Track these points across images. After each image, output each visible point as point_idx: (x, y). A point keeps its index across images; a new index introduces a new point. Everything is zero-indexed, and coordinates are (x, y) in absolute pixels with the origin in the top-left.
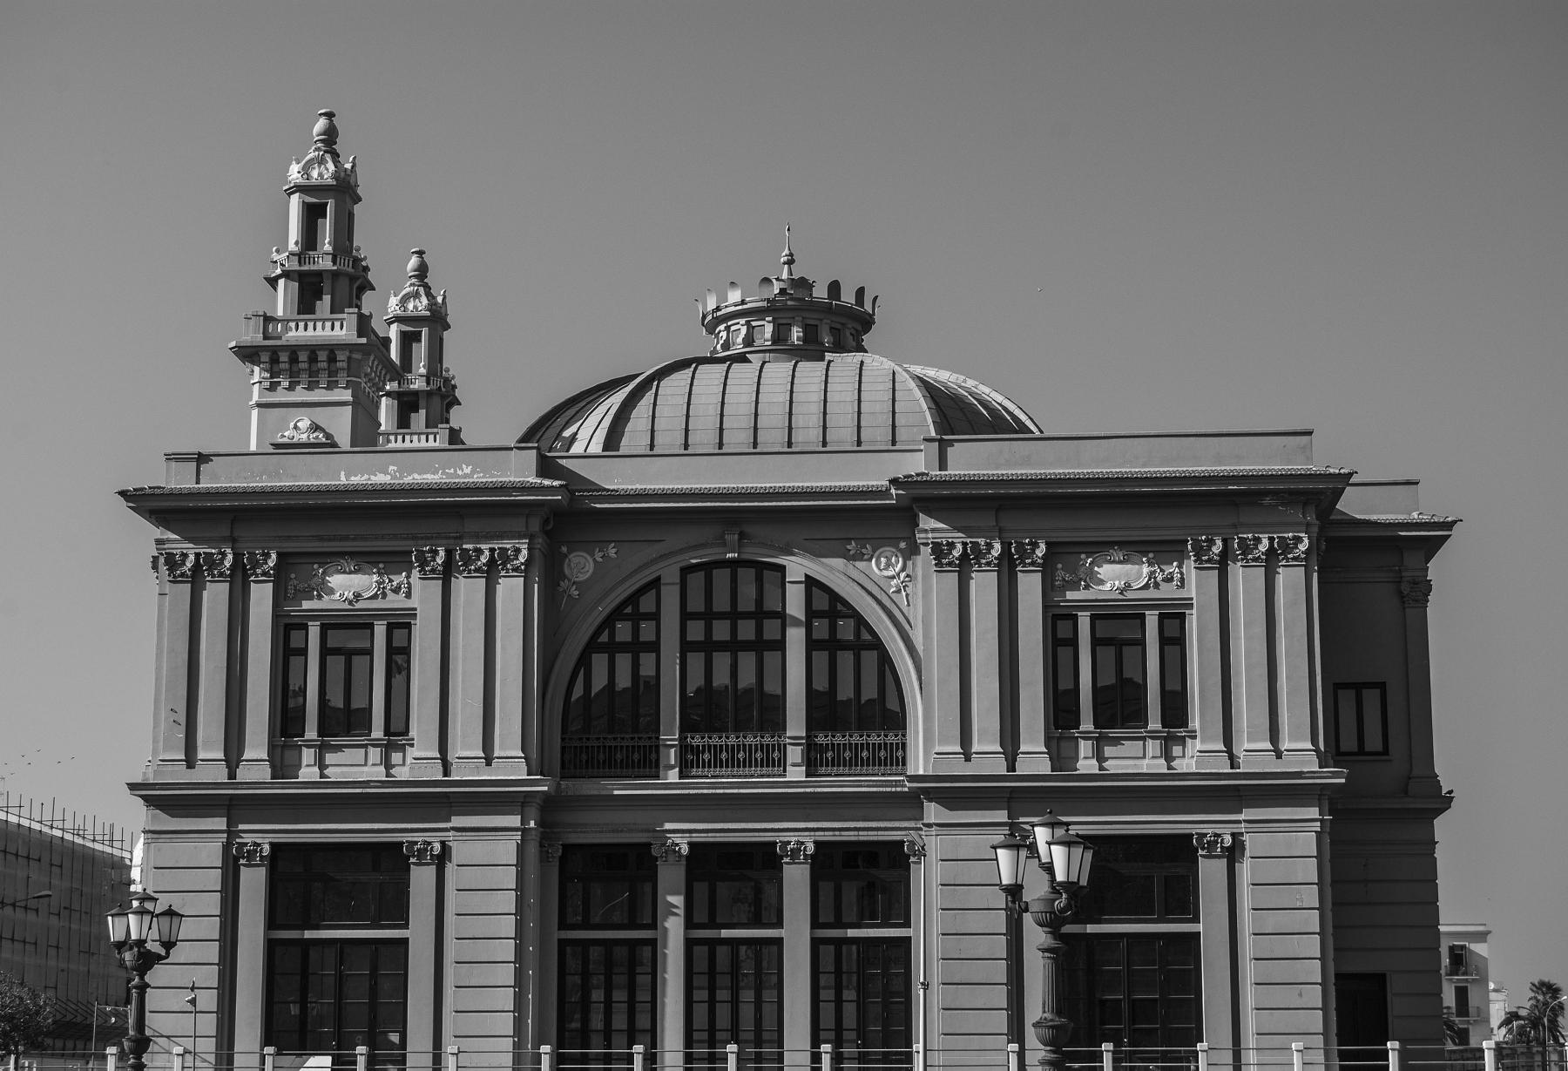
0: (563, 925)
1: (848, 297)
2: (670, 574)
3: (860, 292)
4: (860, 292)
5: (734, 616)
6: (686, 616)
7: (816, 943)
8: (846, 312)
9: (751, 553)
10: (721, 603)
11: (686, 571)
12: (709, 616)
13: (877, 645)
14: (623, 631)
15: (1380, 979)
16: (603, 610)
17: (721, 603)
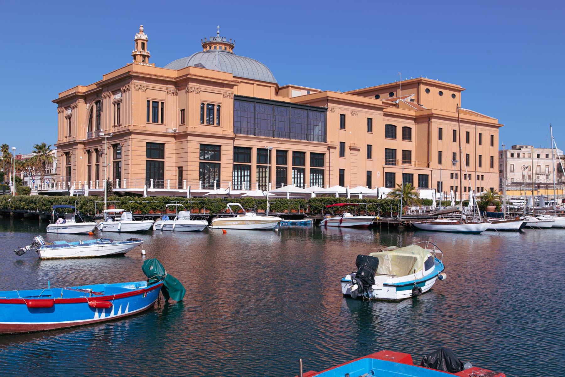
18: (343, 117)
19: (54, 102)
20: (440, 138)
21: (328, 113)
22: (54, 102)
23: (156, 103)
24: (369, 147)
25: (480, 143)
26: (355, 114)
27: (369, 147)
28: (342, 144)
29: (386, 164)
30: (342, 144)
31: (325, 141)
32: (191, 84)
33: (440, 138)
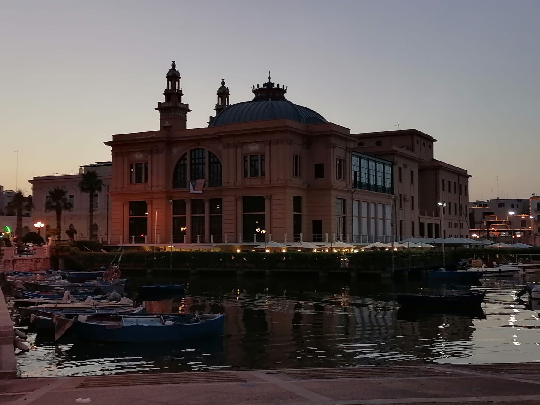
0: (174, 214)
1: (281, 87)
2: (188, 152)
3: (283, 86)
4: (283, 86)
5: (199, 158)
6: (191, 158)
7: (174, 218)
8: (281, 90)
9: (200, 147)
10: (197, 156)
11: (191, 151)
12: (195, 159)
13: (220, 163)
14: (182, 162)
15: (321, 221)
16: (177, 160)
17: (197, 156)
18: (400, 169)
19: (107, 143)
20: (443, 190)
21: (394, 166)
22: (107, 143)
23: (296, 157)
24: (413, 197)
25: (461, 194)
26: (405, 166)
27: (413, 197)
28: (401, 195)
29: (420, 215)
30: (401, 195)
31: (393, 193)
32: (333, 140)
33: (443, 190)
